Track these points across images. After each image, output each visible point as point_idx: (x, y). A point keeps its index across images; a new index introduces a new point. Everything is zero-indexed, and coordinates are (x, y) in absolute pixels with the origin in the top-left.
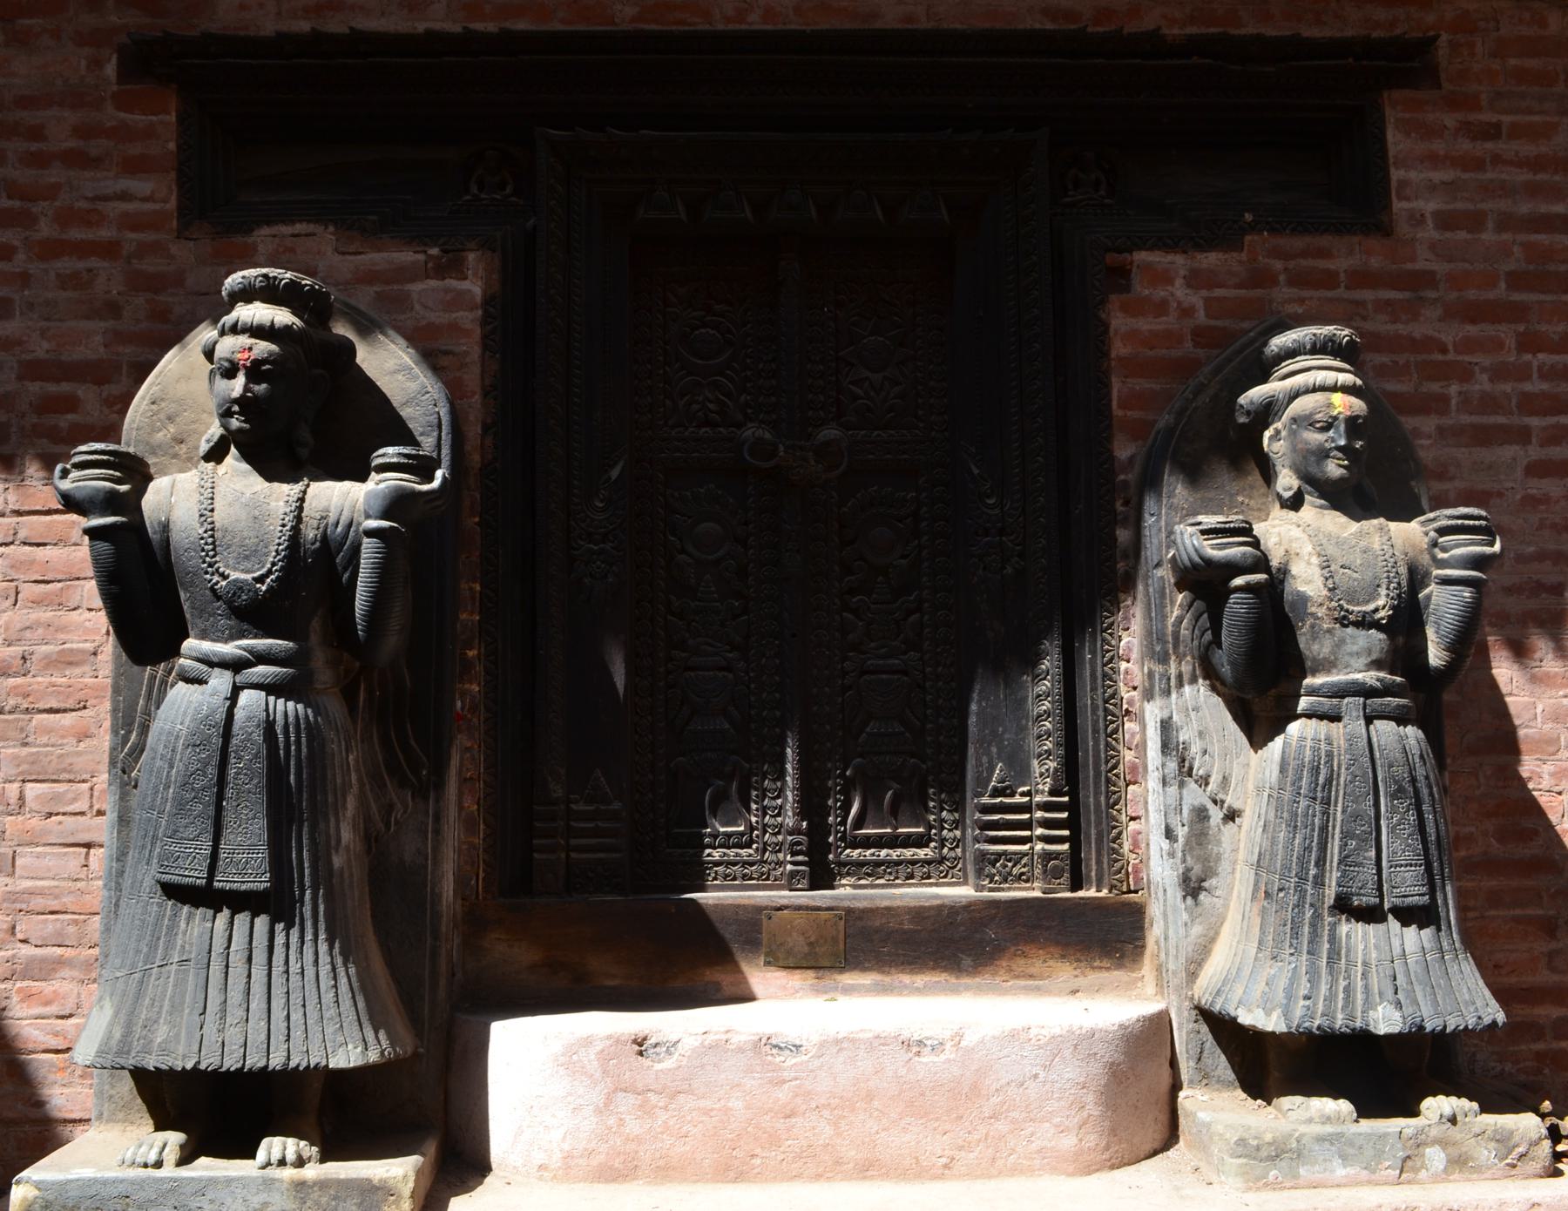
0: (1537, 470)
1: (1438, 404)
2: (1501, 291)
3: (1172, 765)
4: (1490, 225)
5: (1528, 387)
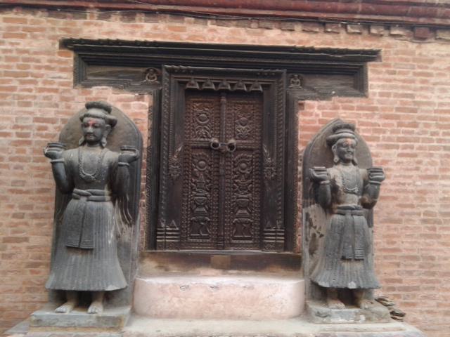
0: (401, 155)
2: (394, 112)
3: (308, 223)
4: (392, 96)
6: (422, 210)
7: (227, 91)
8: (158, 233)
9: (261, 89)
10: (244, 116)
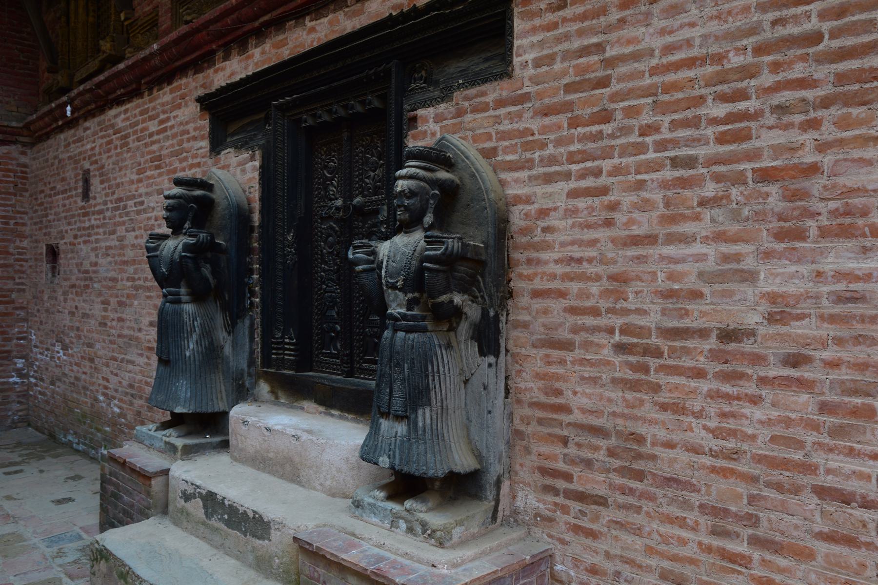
0: (574, 194)
1: (528, 164)
2: (562, 97)
5: (572, 148)
6: (618, 322)
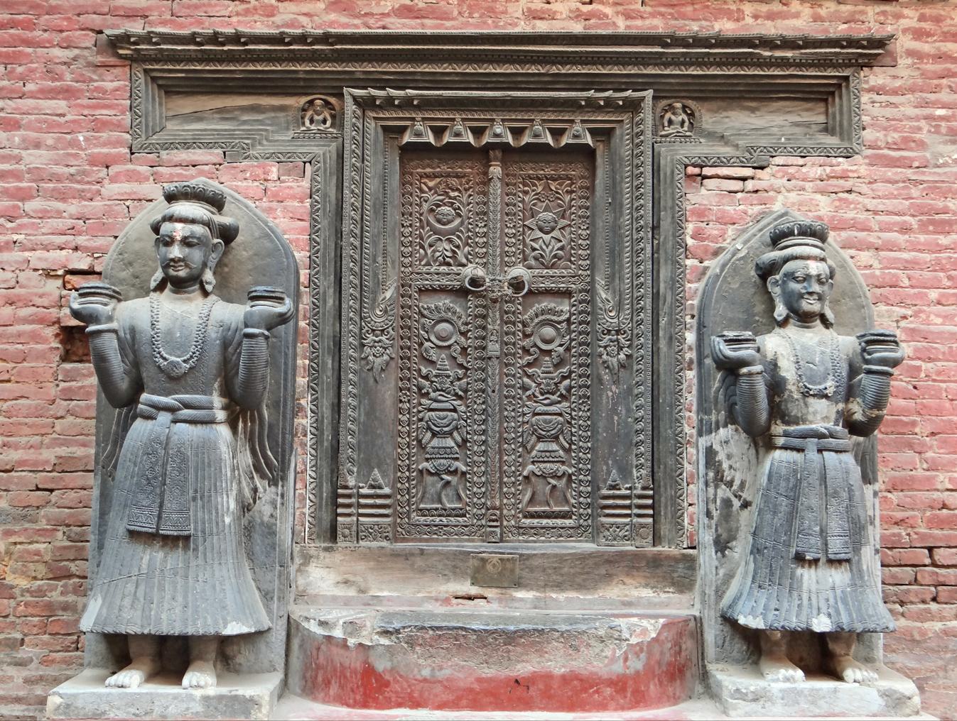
7: (505, 147)
8: (340, 501)
9: (589, 140)
10: (547, 209)
